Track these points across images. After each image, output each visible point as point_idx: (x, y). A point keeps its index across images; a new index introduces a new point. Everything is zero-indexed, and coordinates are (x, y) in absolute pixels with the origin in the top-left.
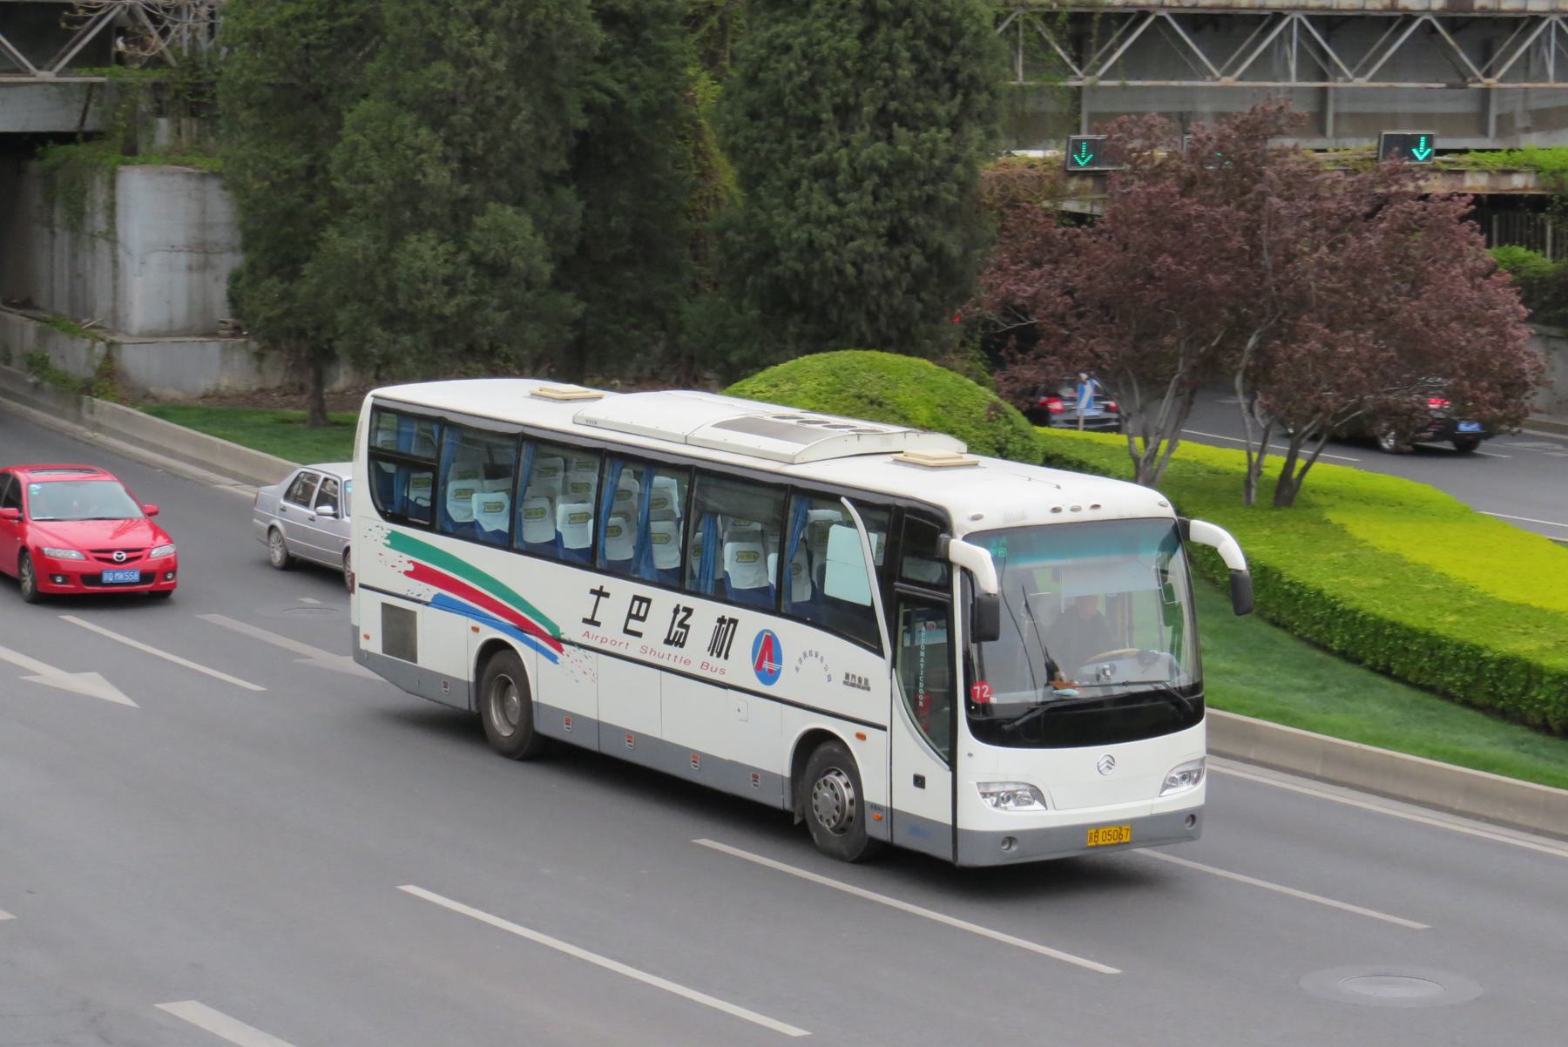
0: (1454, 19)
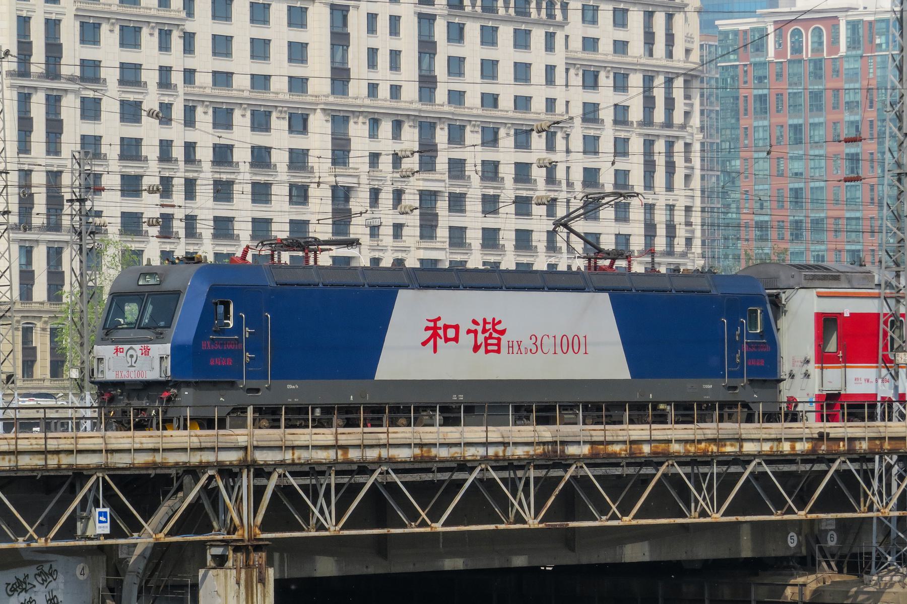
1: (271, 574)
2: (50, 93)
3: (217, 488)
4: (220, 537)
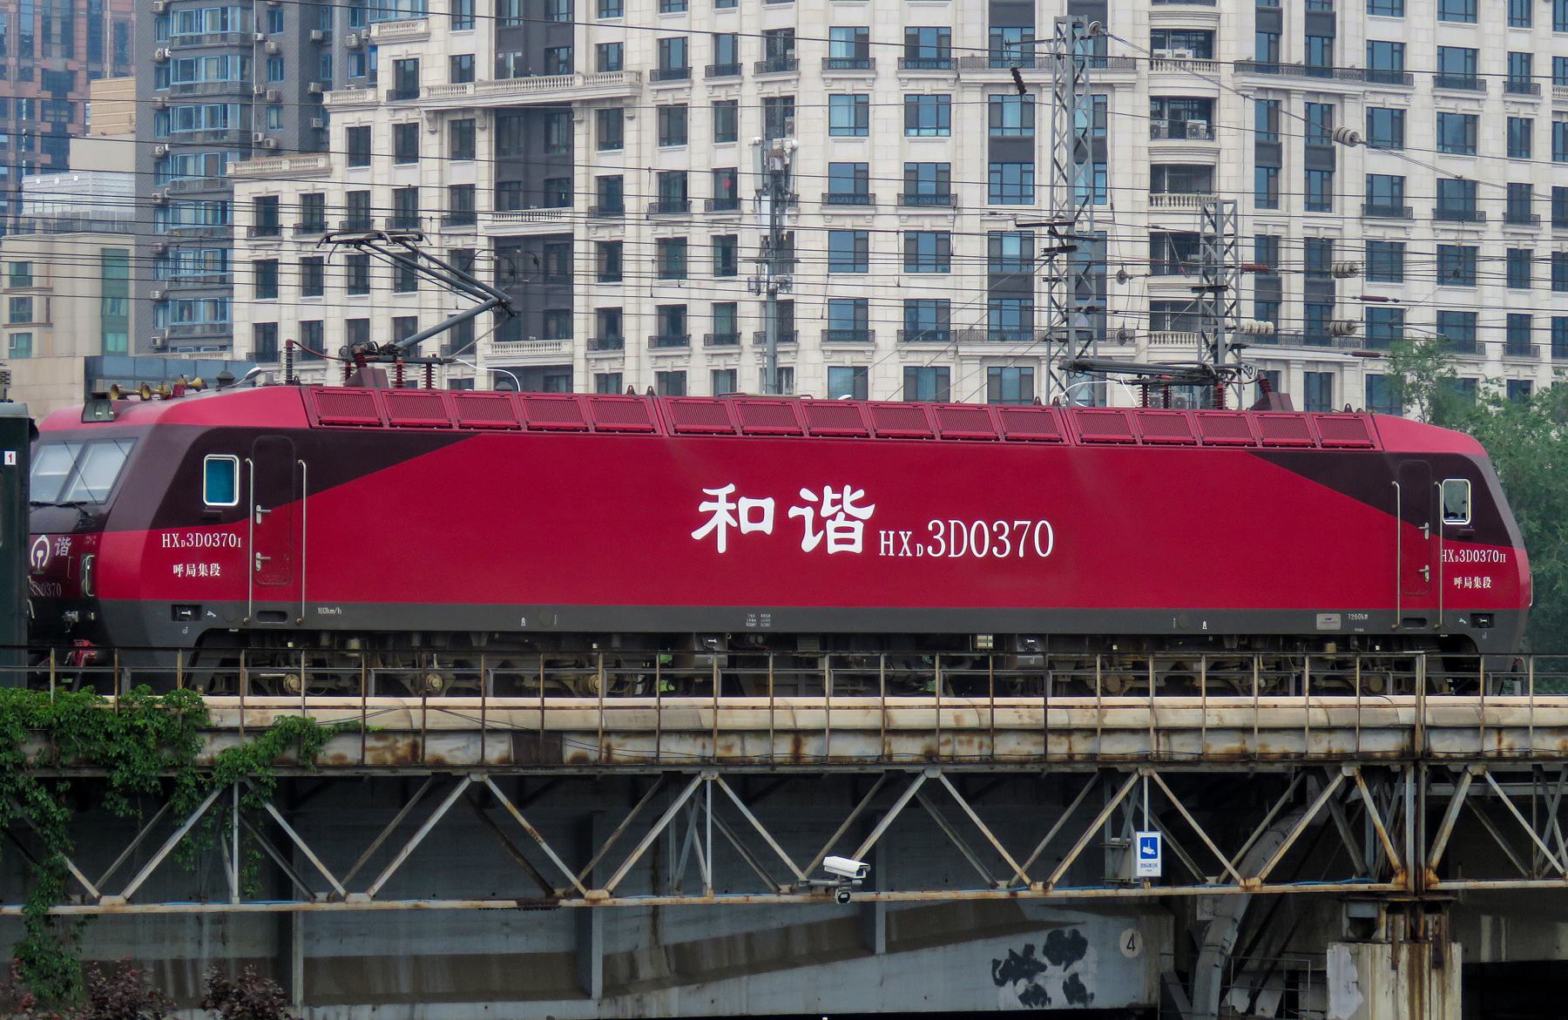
0: (521, 779)
1: (1456, 952)
2: (1312, 100)
3: (1360, 801)
4: (1364, 887)
